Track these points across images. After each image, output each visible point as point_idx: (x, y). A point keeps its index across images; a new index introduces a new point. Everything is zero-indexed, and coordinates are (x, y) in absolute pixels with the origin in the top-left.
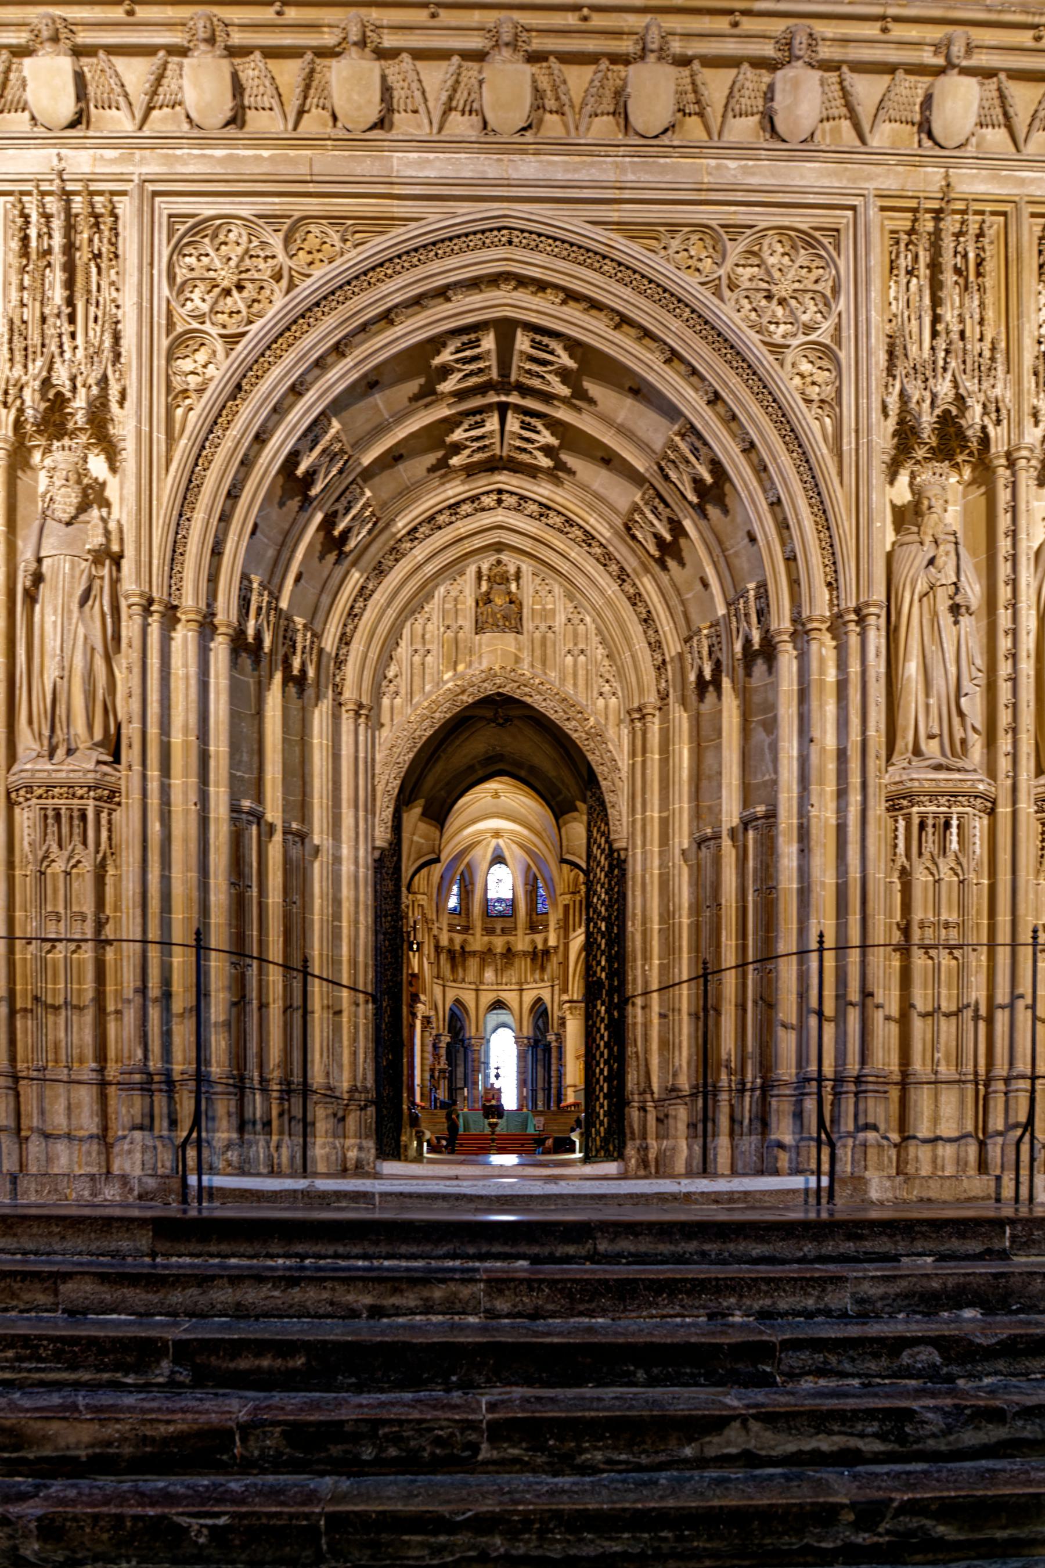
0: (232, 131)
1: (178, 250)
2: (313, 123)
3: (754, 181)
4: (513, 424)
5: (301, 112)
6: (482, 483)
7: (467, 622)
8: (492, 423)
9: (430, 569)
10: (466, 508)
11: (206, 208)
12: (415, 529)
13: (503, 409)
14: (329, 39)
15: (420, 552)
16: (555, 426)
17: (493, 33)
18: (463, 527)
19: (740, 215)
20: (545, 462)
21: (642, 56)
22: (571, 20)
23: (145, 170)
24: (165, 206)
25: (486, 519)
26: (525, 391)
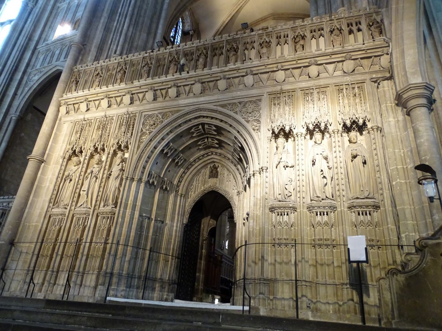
0: (154, 101)
1: (145, 120)
2: (167, 98)
3: (243, 94)
4: (210, 140)
5: (165, 97)
6: (207, 151)
7: (207, 177)
8: (206, 140)
9: (199, 167)
11: (150, 113)
12: (195, 160)
13: (208, 138)
14: (170, 86)
15: (196, 165)
16: (217, 140)
17: (195, 81)
18: (205, 159)
19: (242, 100)
20: (217, 146)
21: (221, 79)
22: (209, 76)
23: (141, 109)
24: (144, 114)
26: (210, 134)
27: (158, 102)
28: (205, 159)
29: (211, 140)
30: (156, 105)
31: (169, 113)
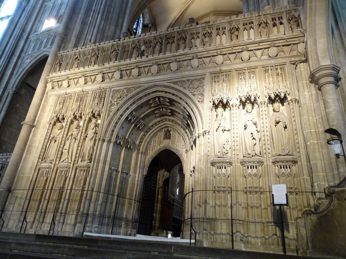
0: (121, 79)
1: (114, 94)
2: (131, 77)
4: (164, 109)
5: (129, 76)
6: (162, 118)
8: (161, 110)
9: (156, 131)
10: (161, 122)
11: (117, 88)
12: (153, 125)
13: (162, 108)
14: (133, 67)
15: (154, 129)
16: (170, 109)
17: (153, 63)
18: (161, 124)
19: (189, 78)
20: (170, 114)
23: (110, 85)
24: (113, 89)
25: (164, 123)
26: (165, 105)
27: (124, 80)
28: (161, 124)
29: (165, 110)
30: (122, 82)
31: (133, 88)
